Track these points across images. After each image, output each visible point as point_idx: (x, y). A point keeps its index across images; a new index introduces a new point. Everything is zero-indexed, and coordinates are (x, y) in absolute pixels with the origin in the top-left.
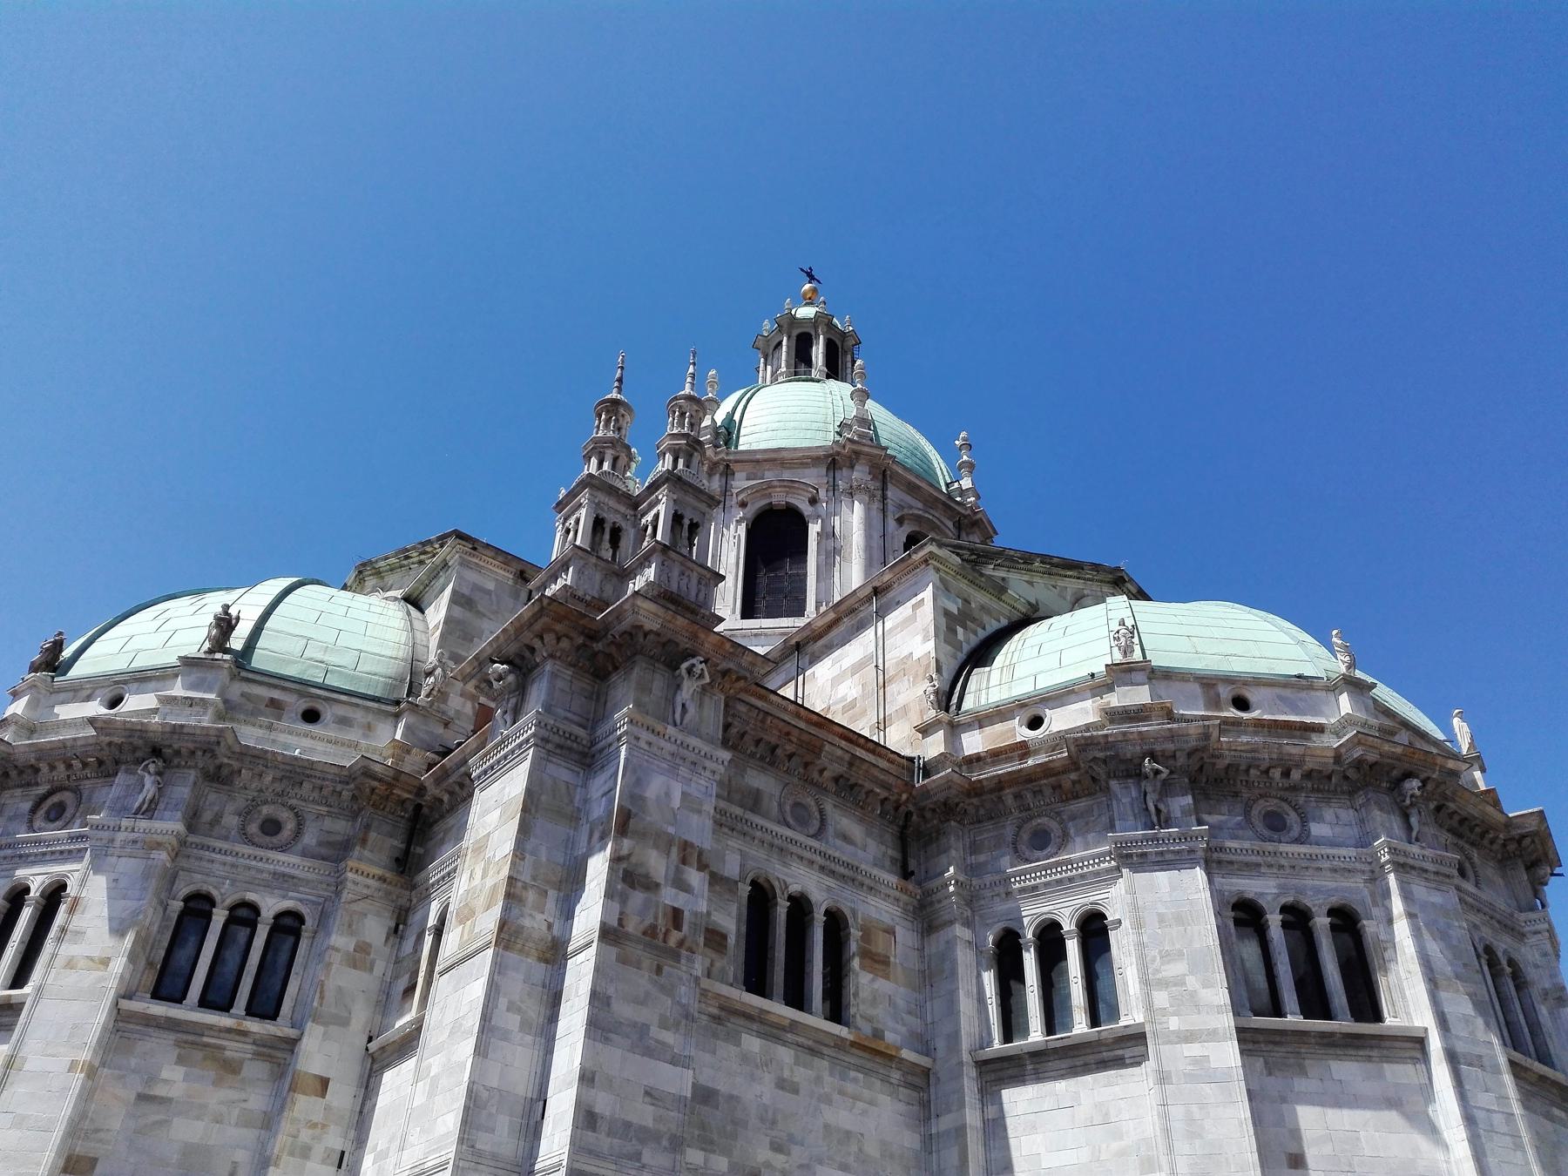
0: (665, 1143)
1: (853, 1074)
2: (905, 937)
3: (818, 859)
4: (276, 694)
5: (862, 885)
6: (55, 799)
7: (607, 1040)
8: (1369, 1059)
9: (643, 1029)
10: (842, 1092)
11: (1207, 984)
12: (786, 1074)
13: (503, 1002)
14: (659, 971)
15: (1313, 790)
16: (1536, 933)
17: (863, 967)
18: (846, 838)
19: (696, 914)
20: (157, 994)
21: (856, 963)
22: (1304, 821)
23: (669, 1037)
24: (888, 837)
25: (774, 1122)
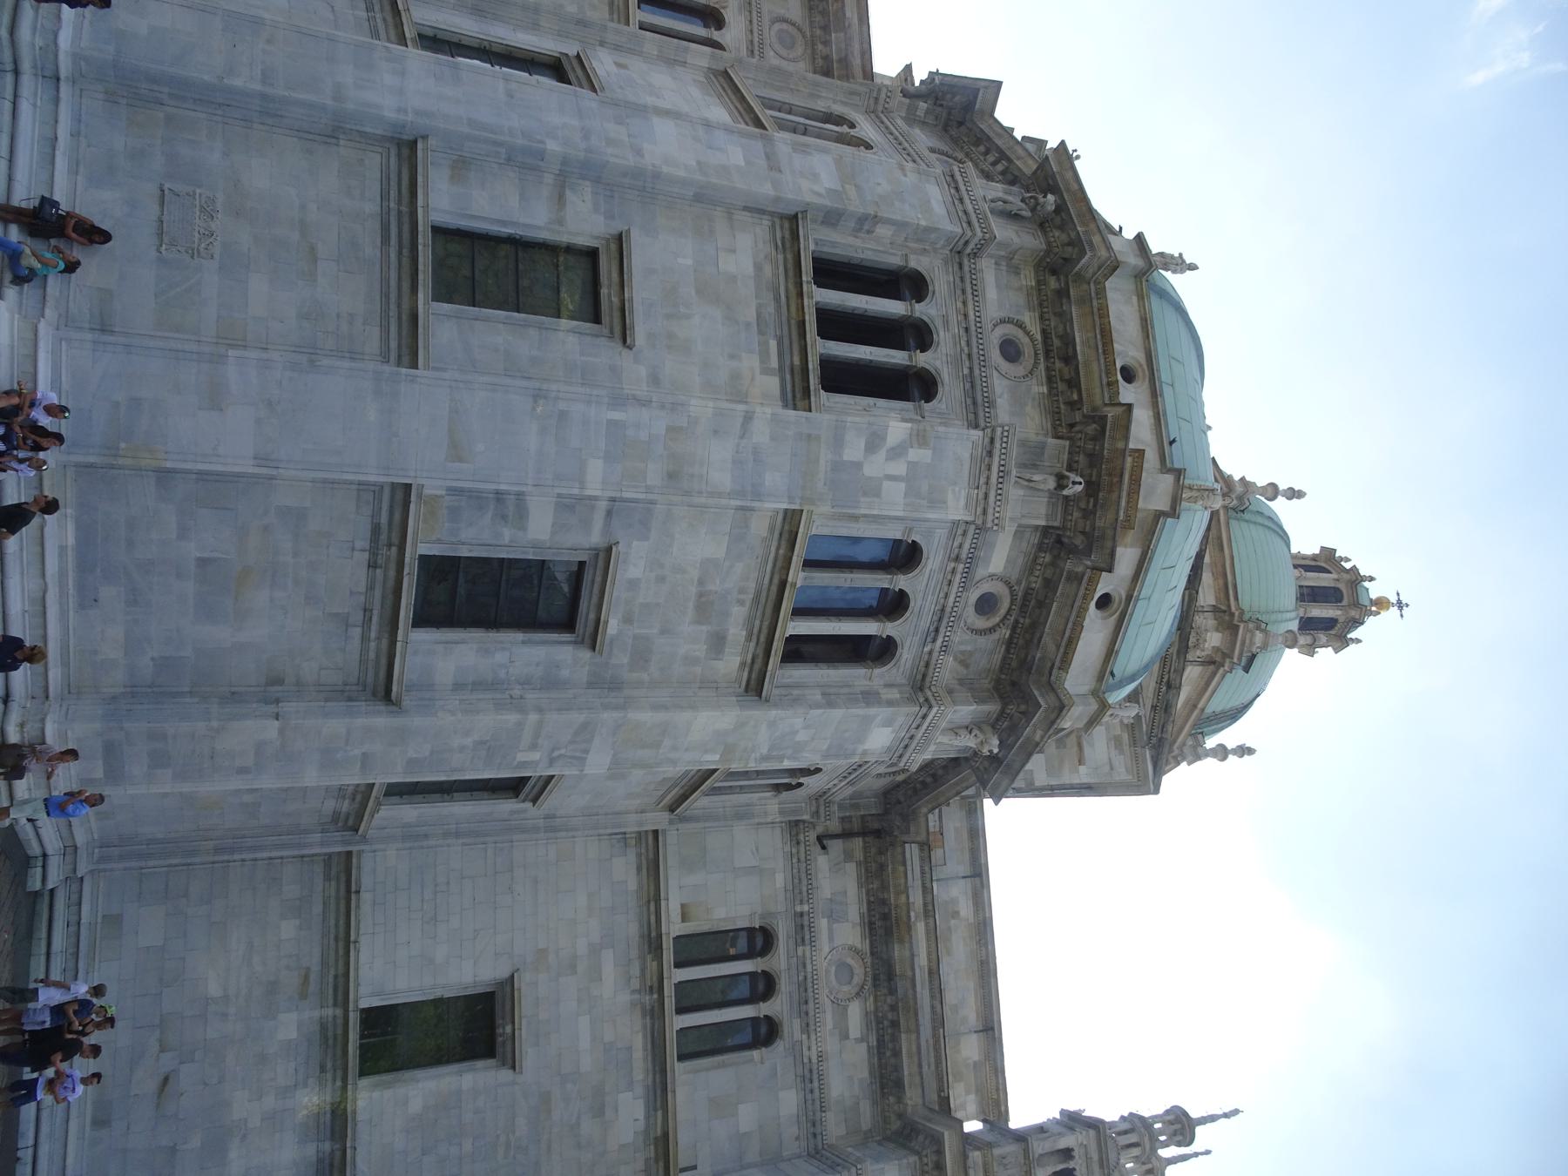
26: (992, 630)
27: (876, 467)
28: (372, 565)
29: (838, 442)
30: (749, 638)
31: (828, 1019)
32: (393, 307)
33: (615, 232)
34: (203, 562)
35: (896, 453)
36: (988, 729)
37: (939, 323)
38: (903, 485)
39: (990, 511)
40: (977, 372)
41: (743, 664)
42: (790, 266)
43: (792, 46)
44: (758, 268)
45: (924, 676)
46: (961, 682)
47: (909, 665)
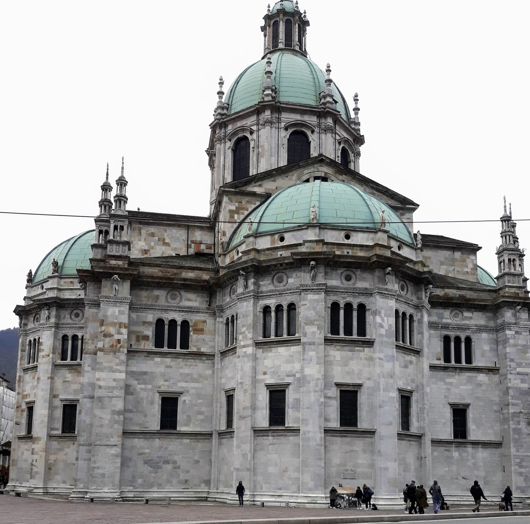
0: (119, 389)
2: (210, 321)
3: (178, 309)
4: (72, 280)
5: (194, 311)
7: (102, 371)
8: (288, 346)
11: (249, 333)
12: (168, 364)
14: (115, 354)
15: (290, 268)
16: (375, 293)
17: (193, 333)
18: (189, 300)
20: (62, 360)
21: (191, 333)
22: (288, 277)
24: (205, 295)
26: (407, 286)
27: (386, 326)
28: (403, 440)
29: (381, 335)
30: (410, 355)
32: (361, 435)
33: (335, 386)
34: (404, 471)
35: (383, 320)
36: (426, 287)
37: (345, 300)
38: (389, 318)
39: (393, 294)
40: (358, 292)
41: (414, 356)
42: (336, 342)
43: (175, 295)
44: (338, 350)
45: (416, 306)
46: (416, 294)
47: (414, 310)
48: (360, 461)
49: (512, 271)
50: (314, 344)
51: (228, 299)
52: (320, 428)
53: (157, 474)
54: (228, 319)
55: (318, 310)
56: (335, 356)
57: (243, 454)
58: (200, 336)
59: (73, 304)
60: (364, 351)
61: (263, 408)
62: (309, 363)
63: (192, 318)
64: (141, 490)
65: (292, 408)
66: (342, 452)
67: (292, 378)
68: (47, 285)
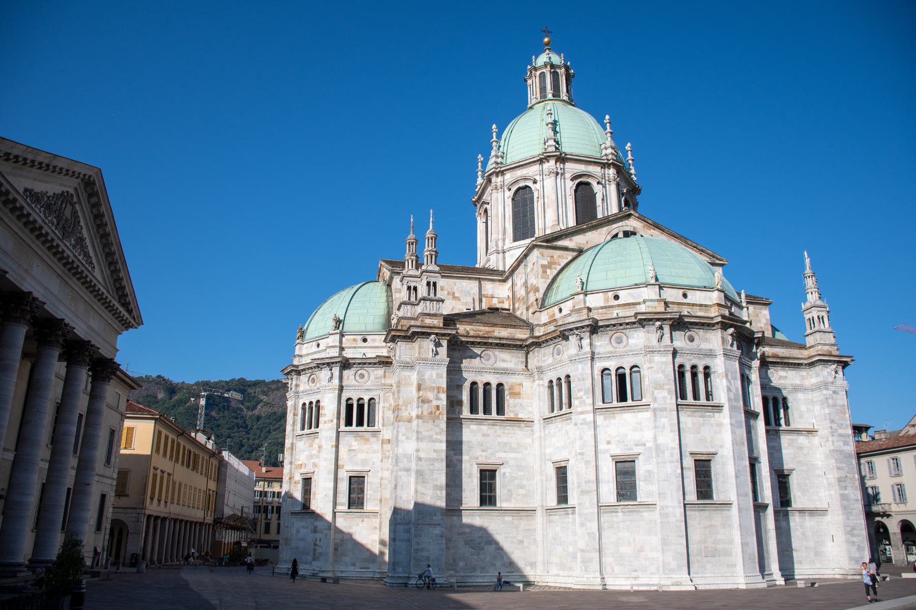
1: (507, 428)
2: (527, 383)
3: (493, 371)
4: (354, 337)
6: (312, 377)
7: (422, 441)
8: (634, 412)
9: (431, 437)
10: (504, 433)
11: (588, 398)
12: (485, 432)
13: (400, 434)
14: (434, 422)
17: (510, 398)
18: (504, 361)
19: (443, 405)
23: (439, 437)
24: (520, 355)
25: (482, 445)
31: (783, 382)
35: (731, 384)
44: (689, 416)
48: (719, 537)
49: (822, 327)
50: (665, 409)
51: (550, 360)
52: (679, 503)
53: (480, 556)
54: (551, 382)
55: (667, 373)
56: (686, 423)
57: (589, 534)
58: (518, 401)
59: (359, 364)
60: (714, 417)
61: (609, 482)
62: (662, 431)
63: (507, 381)
64: (463, 575)
65: (644, 480)
66: (701, 528)
67: (642, 447)
68: (323, 343)
